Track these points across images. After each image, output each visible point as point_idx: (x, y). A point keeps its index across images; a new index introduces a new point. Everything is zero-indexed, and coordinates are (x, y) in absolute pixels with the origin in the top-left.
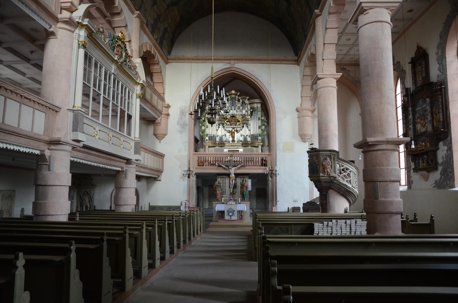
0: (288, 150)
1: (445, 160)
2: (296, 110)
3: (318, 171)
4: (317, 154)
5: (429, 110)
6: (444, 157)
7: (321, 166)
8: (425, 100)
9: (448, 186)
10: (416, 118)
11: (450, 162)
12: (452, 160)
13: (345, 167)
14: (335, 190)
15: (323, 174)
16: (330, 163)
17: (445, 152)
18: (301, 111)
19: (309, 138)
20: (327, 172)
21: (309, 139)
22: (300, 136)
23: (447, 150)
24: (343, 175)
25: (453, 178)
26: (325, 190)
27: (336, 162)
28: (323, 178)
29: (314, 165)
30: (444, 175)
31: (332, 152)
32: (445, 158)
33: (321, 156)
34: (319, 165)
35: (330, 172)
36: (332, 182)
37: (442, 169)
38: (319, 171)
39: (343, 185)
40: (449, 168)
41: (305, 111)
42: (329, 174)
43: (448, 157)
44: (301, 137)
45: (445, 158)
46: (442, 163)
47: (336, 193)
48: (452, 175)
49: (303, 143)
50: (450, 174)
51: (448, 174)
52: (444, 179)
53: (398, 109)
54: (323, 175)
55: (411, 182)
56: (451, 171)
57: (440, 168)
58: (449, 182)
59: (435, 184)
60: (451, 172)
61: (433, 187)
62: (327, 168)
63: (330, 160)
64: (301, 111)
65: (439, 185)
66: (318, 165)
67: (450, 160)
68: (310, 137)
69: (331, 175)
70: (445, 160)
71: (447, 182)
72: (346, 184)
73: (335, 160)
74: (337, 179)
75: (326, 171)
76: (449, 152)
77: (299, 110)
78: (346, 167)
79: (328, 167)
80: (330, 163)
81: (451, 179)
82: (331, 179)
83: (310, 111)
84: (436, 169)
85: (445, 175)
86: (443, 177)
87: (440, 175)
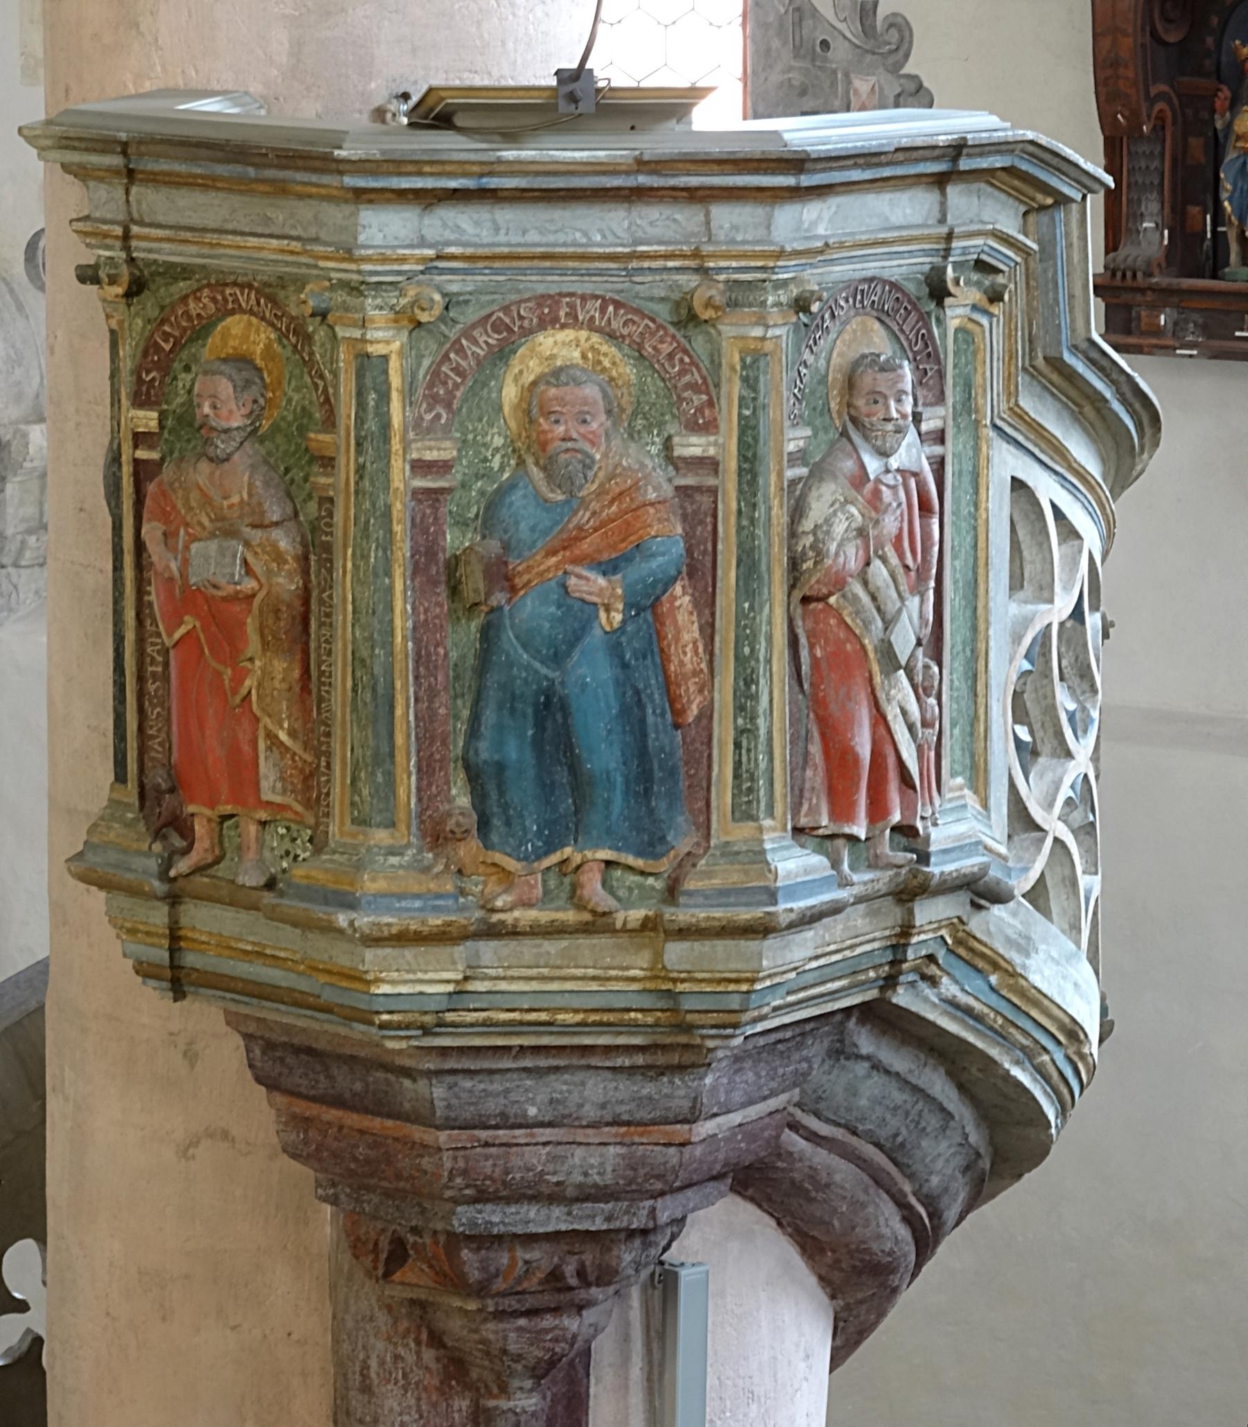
3: (701, 756)
34: (728, 575)
38: (723, 796)
66: (681, 598)
73: (991, 402)
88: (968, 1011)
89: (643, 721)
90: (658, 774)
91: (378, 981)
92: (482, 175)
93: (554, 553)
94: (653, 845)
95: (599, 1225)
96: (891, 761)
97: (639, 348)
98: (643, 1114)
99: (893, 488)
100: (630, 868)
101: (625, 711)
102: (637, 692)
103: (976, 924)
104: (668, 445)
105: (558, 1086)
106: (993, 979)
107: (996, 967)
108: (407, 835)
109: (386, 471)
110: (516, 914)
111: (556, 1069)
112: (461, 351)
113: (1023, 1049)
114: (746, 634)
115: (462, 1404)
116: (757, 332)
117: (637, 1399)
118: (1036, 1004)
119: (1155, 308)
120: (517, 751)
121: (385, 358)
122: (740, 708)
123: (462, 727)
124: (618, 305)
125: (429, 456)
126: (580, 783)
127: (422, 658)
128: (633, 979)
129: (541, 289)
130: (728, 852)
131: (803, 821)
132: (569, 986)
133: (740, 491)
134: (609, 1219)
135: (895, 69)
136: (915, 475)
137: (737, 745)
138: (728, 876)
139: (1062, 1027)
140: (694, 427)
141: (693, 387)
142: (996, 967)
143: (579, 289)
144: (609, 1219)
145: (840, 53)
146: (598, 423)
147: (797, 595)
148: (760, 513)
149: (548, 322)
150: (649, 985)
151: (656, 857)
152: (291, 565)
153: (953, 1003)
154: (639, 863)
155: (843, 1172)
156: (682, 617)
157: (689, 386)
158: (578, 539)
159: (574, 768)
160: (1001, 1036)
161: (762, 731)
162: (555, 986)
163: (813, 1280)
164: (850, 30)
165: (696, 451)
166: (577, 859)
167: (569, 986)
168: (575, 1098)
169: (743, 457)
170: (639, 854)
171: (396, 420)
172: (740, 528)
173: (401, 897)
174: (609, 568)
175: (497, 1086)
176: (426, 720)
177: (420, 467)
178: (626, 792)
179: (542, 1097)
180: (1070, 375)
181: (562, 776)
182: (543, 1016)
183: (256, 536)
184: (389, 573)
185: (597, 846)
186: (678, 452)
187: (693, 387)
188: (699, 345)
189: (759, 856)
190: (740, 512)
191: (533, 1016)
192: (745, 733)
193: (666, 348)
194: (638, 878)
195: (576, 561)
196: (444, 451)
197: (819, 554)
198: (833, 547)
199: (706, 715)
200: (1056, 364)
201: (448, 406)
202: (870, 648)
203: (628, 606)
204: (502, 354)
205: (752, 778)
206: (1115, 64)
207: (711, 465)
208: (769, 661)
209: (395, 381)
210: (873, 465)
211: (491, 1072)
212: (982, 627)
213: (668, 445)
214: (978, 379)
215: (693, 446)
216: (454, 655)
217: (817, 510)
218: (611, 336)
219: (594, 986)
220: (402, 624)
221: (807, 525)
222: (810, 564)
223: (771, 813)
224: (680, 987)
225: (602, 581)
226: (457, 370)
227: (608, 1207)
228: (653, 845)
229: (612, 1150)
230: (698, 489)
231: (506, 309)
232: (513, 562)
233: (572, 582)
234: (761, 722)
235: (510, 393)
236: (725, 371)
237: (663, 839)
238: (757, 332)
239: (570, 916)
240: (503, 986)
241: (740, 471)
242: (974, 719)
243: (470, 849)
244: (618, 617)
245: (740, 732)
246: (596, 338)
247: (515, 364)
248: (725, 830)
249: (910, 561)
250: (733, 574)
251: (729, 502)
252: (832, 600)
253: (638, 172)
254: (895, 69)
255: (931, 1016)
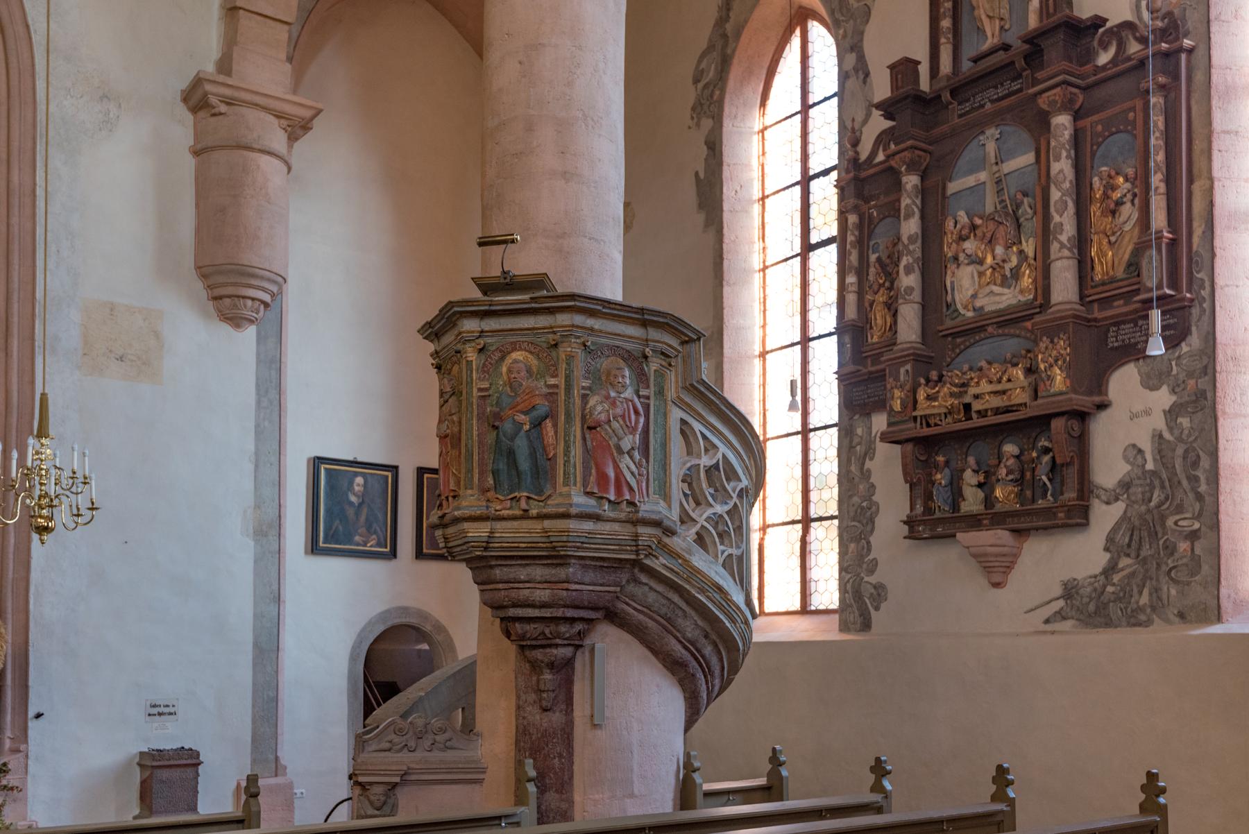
0: (121, 359)
1: (1150, 466)
2: (185, 100)
3: (554, 469)
4: (551, 330)
5: (1071, 182)
6: (1140, 451)
7: (577, 429)
8: (1048, 124)
9: (1171, 613)
10: (948, 238)
11: (1194, 480)
12: (1205, 462)
13: (720, 455)
14: (638, 632)
15: (589, 494)
16: (637, 412)
17: (1159, 423)
18: (223, 108)
19: (267, 298)
20: (620, 481)
21: (266, 305)
22: (204, 276)
23: (1172, 414)
24: (709, 512)
25: (1205, 568)
26: (579, 627)
27: (676, 414)
28: (588, 526)
29: (521, 418)
30: (1139, 549)
31: (653, 334)
32: (1149, 457)
33: (580, 353)
35: (633, 483)
36: (636, 563)
37: (1124, 518)
38: (560, 478)
39: (702, 591)
40: (1180, 509)
41: (252, 115)
42: (631, 503)
43: (1180, 451)
44: (210, 287)
45: (1149, 457)
46: (1125, 485)
47: (638, 649)
48: (1197, 551)
49: (226, 328)
50: (1183, 546)
51: (1171, 549)
52: (1133, 575)
53: (815, 185)
54: (592, 502)
55: (867, 590)
56: (1197, 526)
57: (1105, 516)
58: (1173, 592)
59: (1061, 603)
60: (1193, 536)
61: (1047, 621)
62: (620, 450)
63: (639, 397)
64: (223, 108)
65: (1092, 607)
67: (1196, 464)
68: (273, 295)
69: (643, 507)
70: (1150, 466)
71: (1156, 590)
72: (721, 582)
73: (671, 393)
74: (676, 543)
75: (611, 473)
76: (1184, 421)
77: (213, 100)
78: (724, 456)
79: (626, 444)
80: (637, 412)
81: (1193, 575)
82: (636, 537)
83: (284, 123)
84: (1078, 517)
85: (1146, 551)
86: (1124, 562)
87: (1107, 549)
88: (672, 570)
89: (536, 458)
90: (541, 473)
91: (468, 532)
92: (490, 305)
93: (511, 409)
94: (540, 493)
95: (548, 615)
96: (623, 480)
97: (538, 355)
98: (553, 579)
99: (622, 402)
100: (534, 499)
101: (531, 454)
102: (534, 449)
103: (666, 540)
104: (546, 382)
105: (529, 570)
106: (680, 561)
107: (680, 558)
108: (475, 491)
109: (472, 392)
110: (503, 512)
111: (527, 565)
112: (491, 358)
113: (699, 588)
114: (567, 434)
115: (535, 678)
116: (569, 349)
117: (587, 683)
118: (700, 574)
119: (919, 525)
120: (502, 466)
121: (472, 361)
122: (565, 455)
123: (491, 461)
124: (532, 343)
125: (482, 387)
126: (519, 474)
127: (480, 442)
128: (537, 533)
129: (512, 340)
130: (561, 494)
131: (588, 490)
132: (521, 535)
133: (565, 394)
134: (551, 613)
135: (868, 482)
136: (631, 401)
137: (565, 465)
138: (559, 500)
139: (713, 584)
140: (553, 376)
141: (552, 365)
142: (680, 558)
143: (521, 340)
144: (551, 613)
145: (857, 479)
146: (523, 374)
147: (586, 426)
148: (571, 400)
149: (514, 350)
150: (543, 535)
151: (541, 496)
152: (457, 424)
153: (664, 565)
154: (536, 497)
155: (651, 624)
156: (549, 429)
157: (551, 365)
158: (517, 405)
159: (517, 468)
160: (689, 583)
161: (572, 461)
162: (517, 535)
163: (660, 666)
164: (858, 474)
165: (553, 383)
166: (518, 496)
167: (521, 535)
168: (534, 573)
169: (566, 385)
170: (536, 495)
171: (474, 378)
172: (565, 405)
173: (472, 507)
174: (526, 413)
175: (513, 570)
176: (481, 460)
177: (480, 390)
178: (532, 477)
179: (525, 573)
180: (696, 389)
181: (514, 473)
182: (516, 545)
183: (450, 418)
184: (472, 419)
185: (524, 492)
186: (548, 383)
187: (552, 365)
188: (554, 354)
189: (569, 495)
190: (565, 400)
191: (513, 545)
192: (567, 462)
193: (545, 355)
194: (537, 503)
195: (517, 412)
196: (485, 385)
197: (591, 414)
198: (596, 413)
199: (555, 455)
200: (692, 385)
201: (488, 374)
202: (612, 445)
203: (531, 423)
204: (502, 358)
205: (569, 474)
206: (906, 465)
207: (556, 386)
208: (574, 442)
209: (474, 367)
210: (613, 394)
211: (511, 565)
212: (668, 456)
213: (546, 382)
214: (666, 387)
215: (552, 381)
216: (489, 442)
217: (592, 402)
218: (531, 352)
219: (528, 535)
220: (475, 433)
221: (588, 406)
222: (588, 417)
223: (575, 484)
224: (549, 534)
225: (523, 417)
226: (491, 364)
227: (551, 610)
228: (540, 493)
229: (547, 591)
230: (553, 393)
231: (502, 346)
232: (502, 414)
233: (516, 417)
234: (571, 458)
235: (504, 369)
236: (560, 361)
237: (542, 491)
238: (569, 349)
239: (518, 512)
240: (504, 535)
241: (565, 389)
242: (665, 482)
243: (491, 494)
244: (528, 427)
245: (565, 461)
246: (527, 353)
247: (506, 362)
248: (562, 489)
249: (628, 424)
250: (563, 417)
251: (562, 396)
252: (598, 429)
253: (531, 302)
254: (868, 482)
255: (658, 569)
